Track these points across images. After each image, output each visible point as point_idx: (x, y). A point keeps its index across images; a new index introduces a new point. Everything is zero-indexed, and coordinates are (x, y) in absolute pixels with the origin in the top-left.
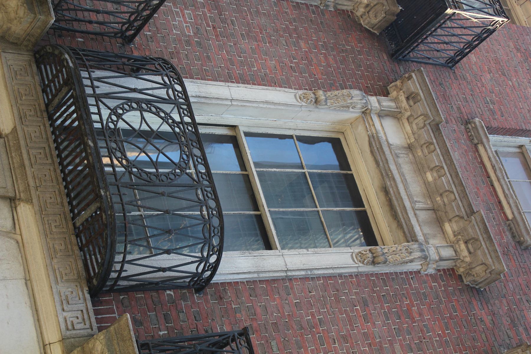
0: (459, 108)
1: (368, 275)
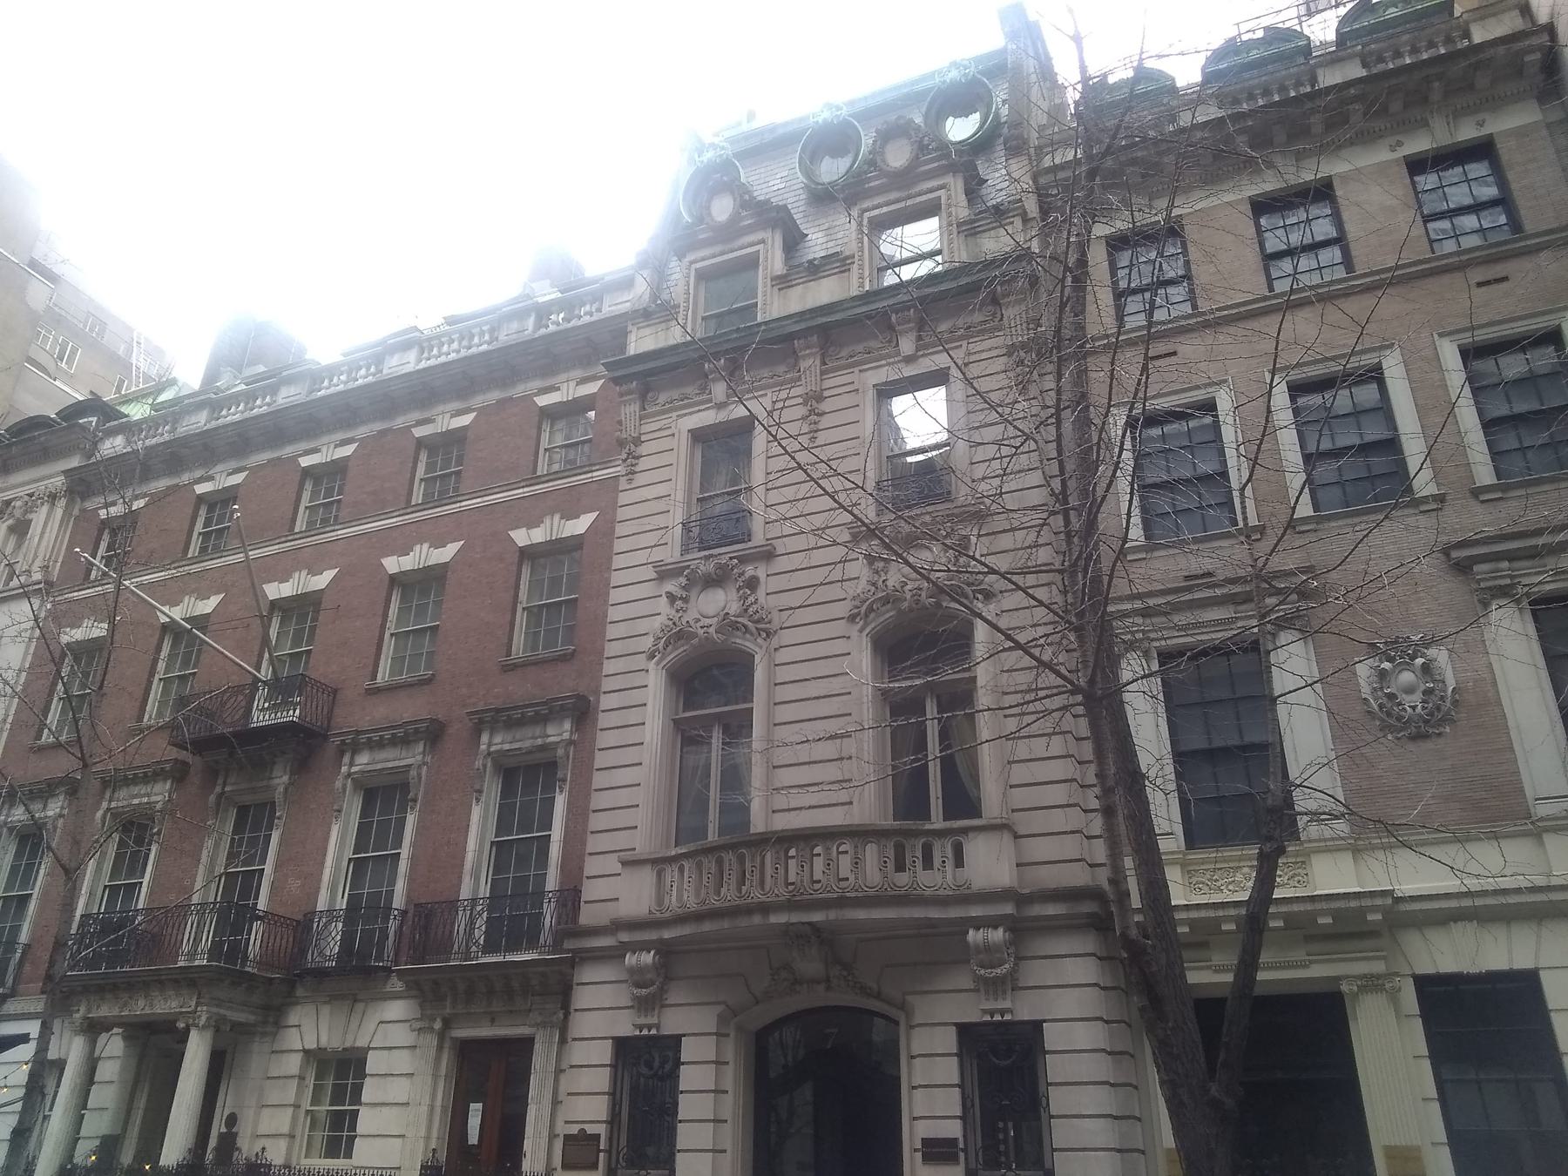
0: (359, 694)
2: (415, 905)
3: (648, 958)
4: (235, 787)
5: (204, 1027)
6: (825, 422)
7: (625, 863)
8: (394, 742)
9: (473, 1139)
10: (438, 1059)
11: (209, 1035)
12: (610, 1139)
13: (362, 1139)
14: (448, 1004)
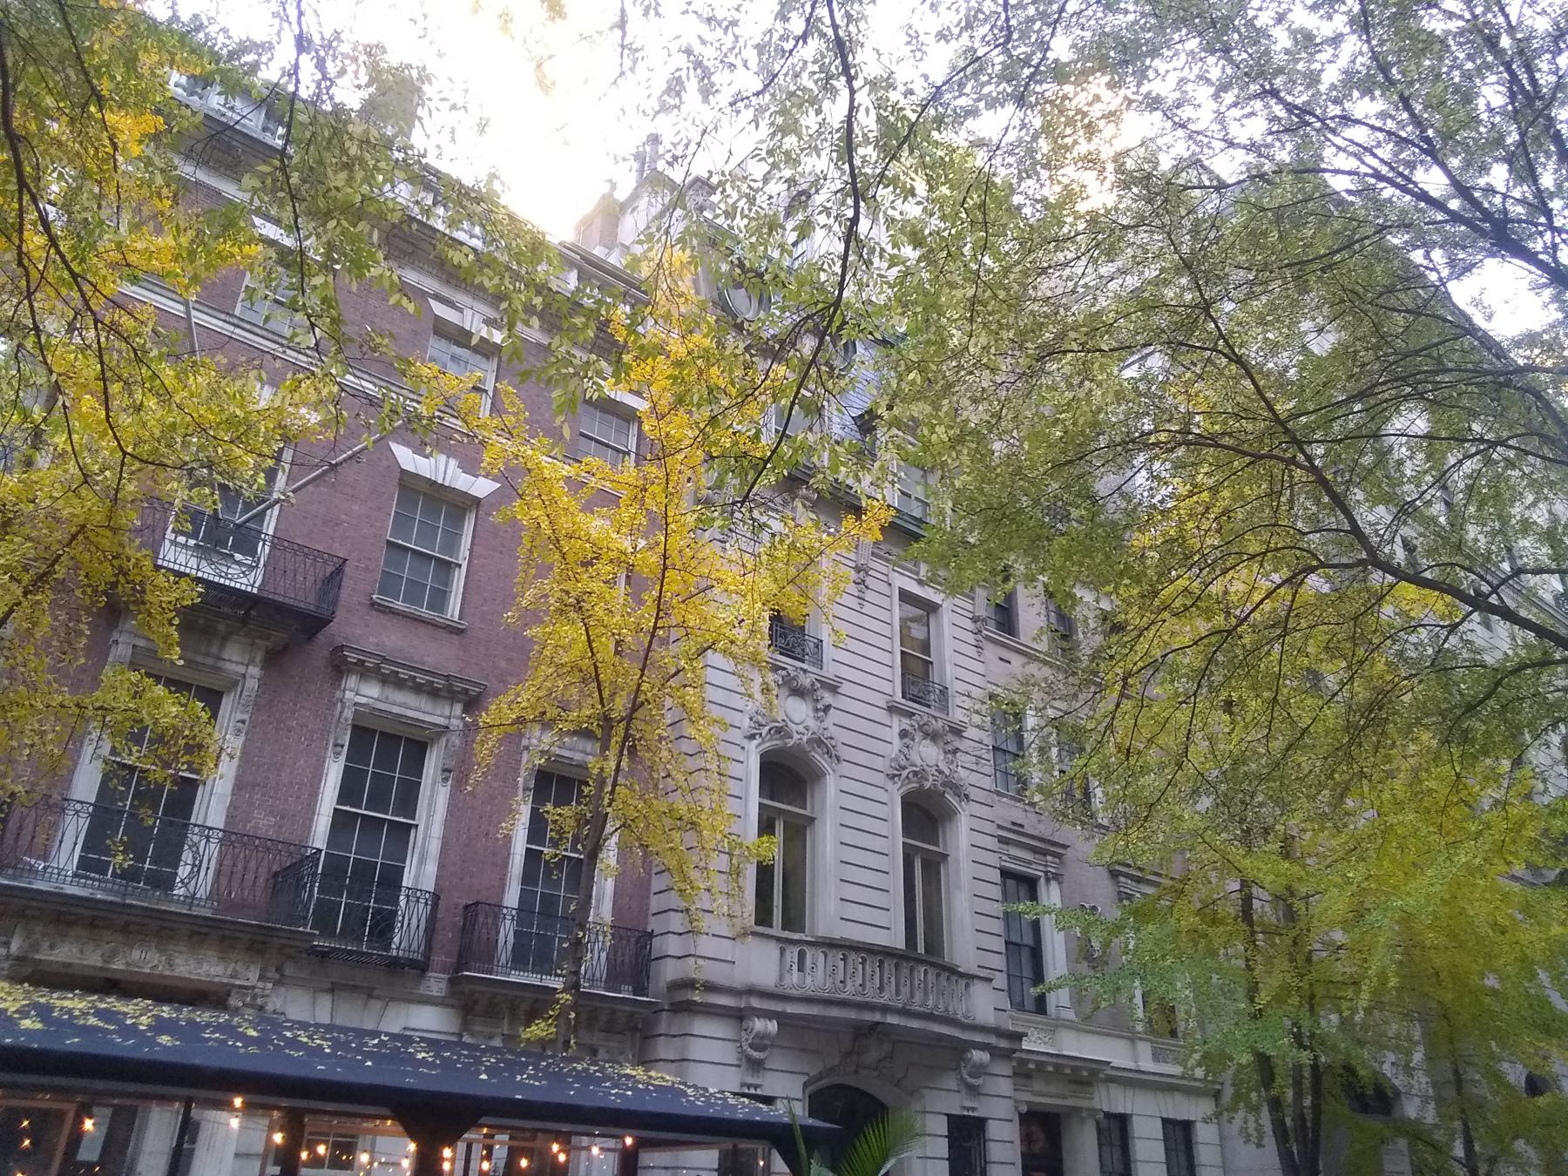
6: (869, 595)
8: (418, 689)
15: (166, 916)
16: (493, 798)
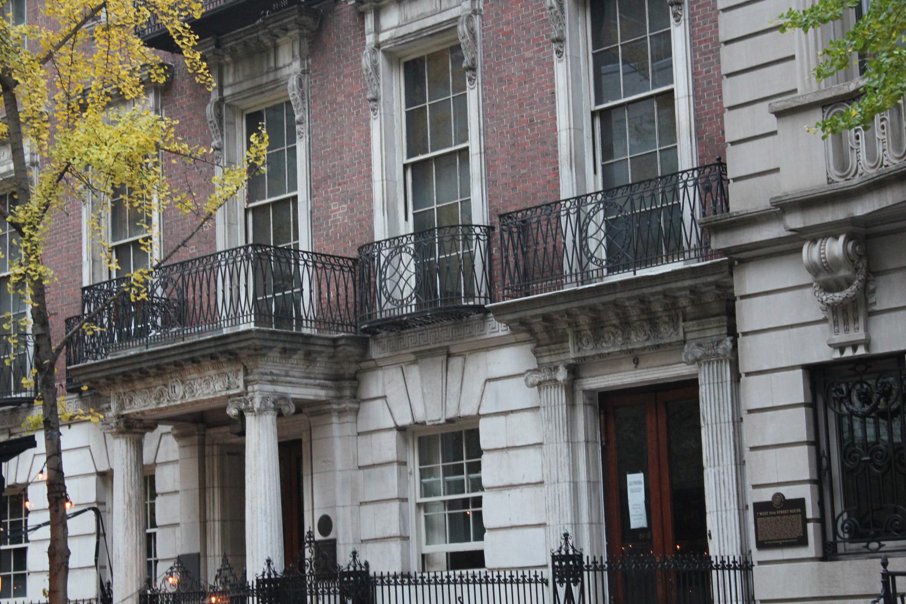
1: (484, 73)
2: (501, 216)
3: (835, 247)
4: (238, 89)
5: (260, 412)
7: (780, 114)
9: (638, 518)
10: (571, 422)
11: (269, 419)
12: (821, 504)
13: (494, 533)
14: (570, 344)
15: (162, 355)
16: (528, 72)
